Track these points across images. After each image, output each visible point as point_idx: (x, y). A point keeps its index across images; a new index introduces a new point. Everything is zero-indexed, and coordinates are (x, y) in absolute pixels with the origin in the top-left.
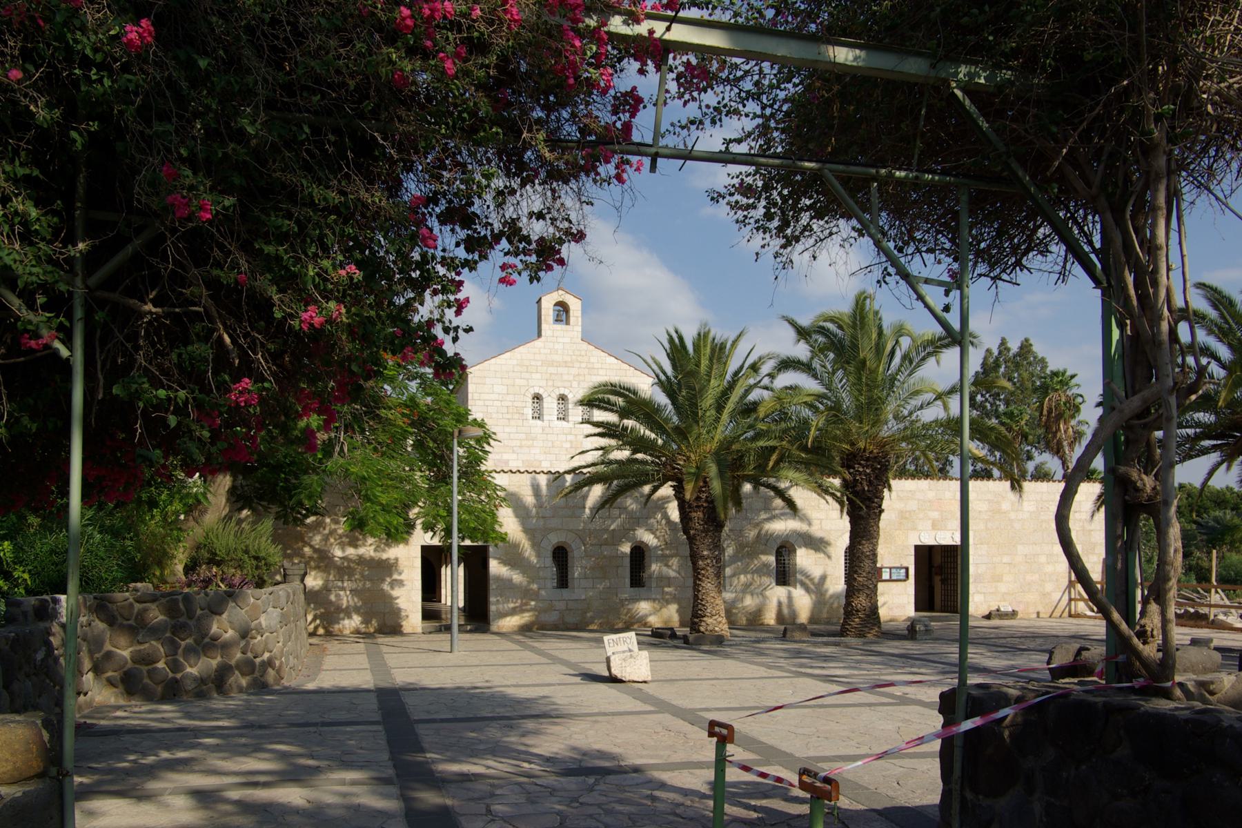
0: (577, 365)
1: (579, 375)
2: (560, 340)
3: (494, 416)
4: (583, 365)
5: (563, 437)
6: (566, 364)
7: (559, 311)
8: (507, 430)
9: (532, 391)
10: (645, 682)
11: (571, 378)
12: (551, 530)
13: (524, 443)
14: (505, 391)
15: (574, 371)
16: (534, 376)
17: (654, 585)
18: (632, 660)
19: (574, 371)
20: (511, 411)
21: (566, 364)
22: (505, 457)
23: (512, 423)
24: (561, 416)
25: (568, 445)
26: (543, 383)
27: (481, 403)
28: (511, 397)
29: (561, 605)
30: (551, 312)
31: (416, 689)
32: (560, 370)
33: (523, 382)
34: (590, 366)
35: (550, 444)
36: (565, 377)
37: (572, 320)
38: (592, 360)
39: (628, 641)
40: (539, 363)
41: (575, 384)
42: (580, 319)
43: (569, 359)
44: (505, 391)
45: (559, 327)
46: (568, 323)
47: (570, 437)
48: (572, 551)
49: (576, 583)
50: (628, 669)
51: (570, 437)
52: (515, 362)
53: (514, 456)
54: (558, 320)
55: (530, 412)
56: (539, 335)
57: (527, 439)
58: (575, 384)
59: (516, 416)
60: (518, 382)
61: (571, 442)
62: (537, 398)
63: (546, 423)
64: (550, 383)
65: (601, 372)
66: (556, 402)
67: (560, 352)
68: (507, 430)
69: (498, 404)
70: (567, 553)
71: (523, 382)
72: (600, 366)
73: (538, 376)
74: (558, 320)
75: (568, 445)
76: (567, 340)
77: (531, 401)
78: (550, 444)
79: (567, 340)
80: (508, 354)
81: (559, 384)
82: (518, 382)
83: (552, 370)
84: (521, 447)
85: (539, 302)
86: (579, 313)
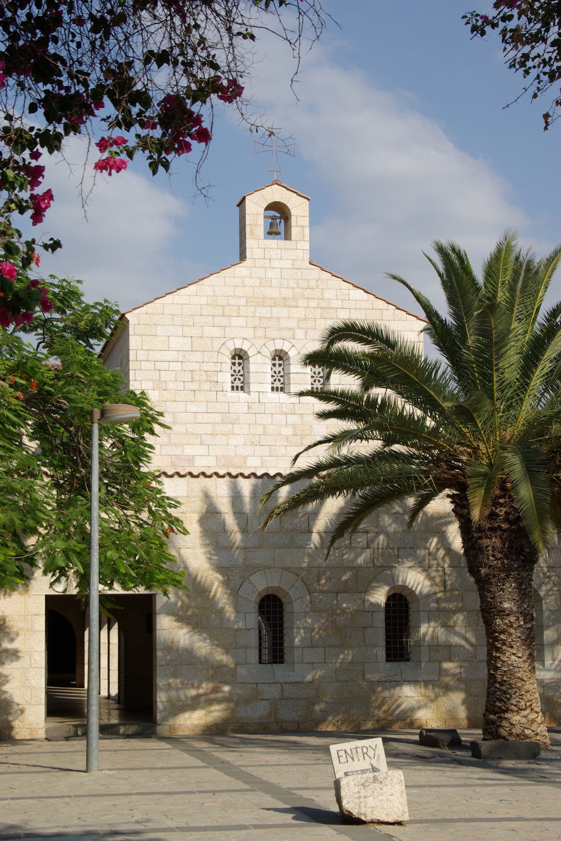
0: (302, 303)
1: (306, 319)
2: (275, 264)
3: (171, 386)
4: (313, 303)
5: (280, 419)
6: (285, 302)
7: (274, 218)
8: (192, 407)
9: (231, 346)
10: (399, 823)
11: (294, 324)
12: (257, 569)
13: (218, 428)
14: (188, 347)
15: (299, 313)
16: (235, 321)
17: (424, 658)
18: (376, 785)
19: (299, 313)
20: (197, 378)
21: (285, 302)
22: (189, 451)
23: (200, 396)
24: (278, 384)
25: (288, 431)
26: (249, 333)
27: (150, 366)
28: (197, 356)
29: (273, 692)
30: (261, 220)
31: (18, 836)
32: (276, 311)
33: (217, 332)
34: (323, 304)
35: (260, 430)
36: (284, 323)
37: (295, 231)
38: (328, 294)
39: (371, 753)
40: (243, 302)
41: (300, 334)
42: (307, 230)
43: (288, 293)
44: (188, 347)
45: (274, 243)
46: (287, 237)
47: (292, 419)
48: (291, 603)
49: (297, 654)
50: (371, 801)
52: (203, 300)
53: (202, 450)
54: (271, 233)
55: (229, 379)
56: (243, 257)
57: (223, 423)
58: (300, 334)
59: (206, 386)
60: (209, 331)
61: (294, 426)
63: (254, 397)
64: (260, 333)
66: (269, 362)
67: (275, 283)
68: (192, 407)
69: (177, 366)
70: (281, 606)
71: (217, 332)
73: (241, 321)
74: (271, 233)
75: (288, 431)
76: (287, 264)
77: (229, 361)
78: (260, 430)
79: (287, 264)
82: (209, 331)
83: (262, 312)
84: (213, 435)
85: (242, 203)
86: (306, 221)
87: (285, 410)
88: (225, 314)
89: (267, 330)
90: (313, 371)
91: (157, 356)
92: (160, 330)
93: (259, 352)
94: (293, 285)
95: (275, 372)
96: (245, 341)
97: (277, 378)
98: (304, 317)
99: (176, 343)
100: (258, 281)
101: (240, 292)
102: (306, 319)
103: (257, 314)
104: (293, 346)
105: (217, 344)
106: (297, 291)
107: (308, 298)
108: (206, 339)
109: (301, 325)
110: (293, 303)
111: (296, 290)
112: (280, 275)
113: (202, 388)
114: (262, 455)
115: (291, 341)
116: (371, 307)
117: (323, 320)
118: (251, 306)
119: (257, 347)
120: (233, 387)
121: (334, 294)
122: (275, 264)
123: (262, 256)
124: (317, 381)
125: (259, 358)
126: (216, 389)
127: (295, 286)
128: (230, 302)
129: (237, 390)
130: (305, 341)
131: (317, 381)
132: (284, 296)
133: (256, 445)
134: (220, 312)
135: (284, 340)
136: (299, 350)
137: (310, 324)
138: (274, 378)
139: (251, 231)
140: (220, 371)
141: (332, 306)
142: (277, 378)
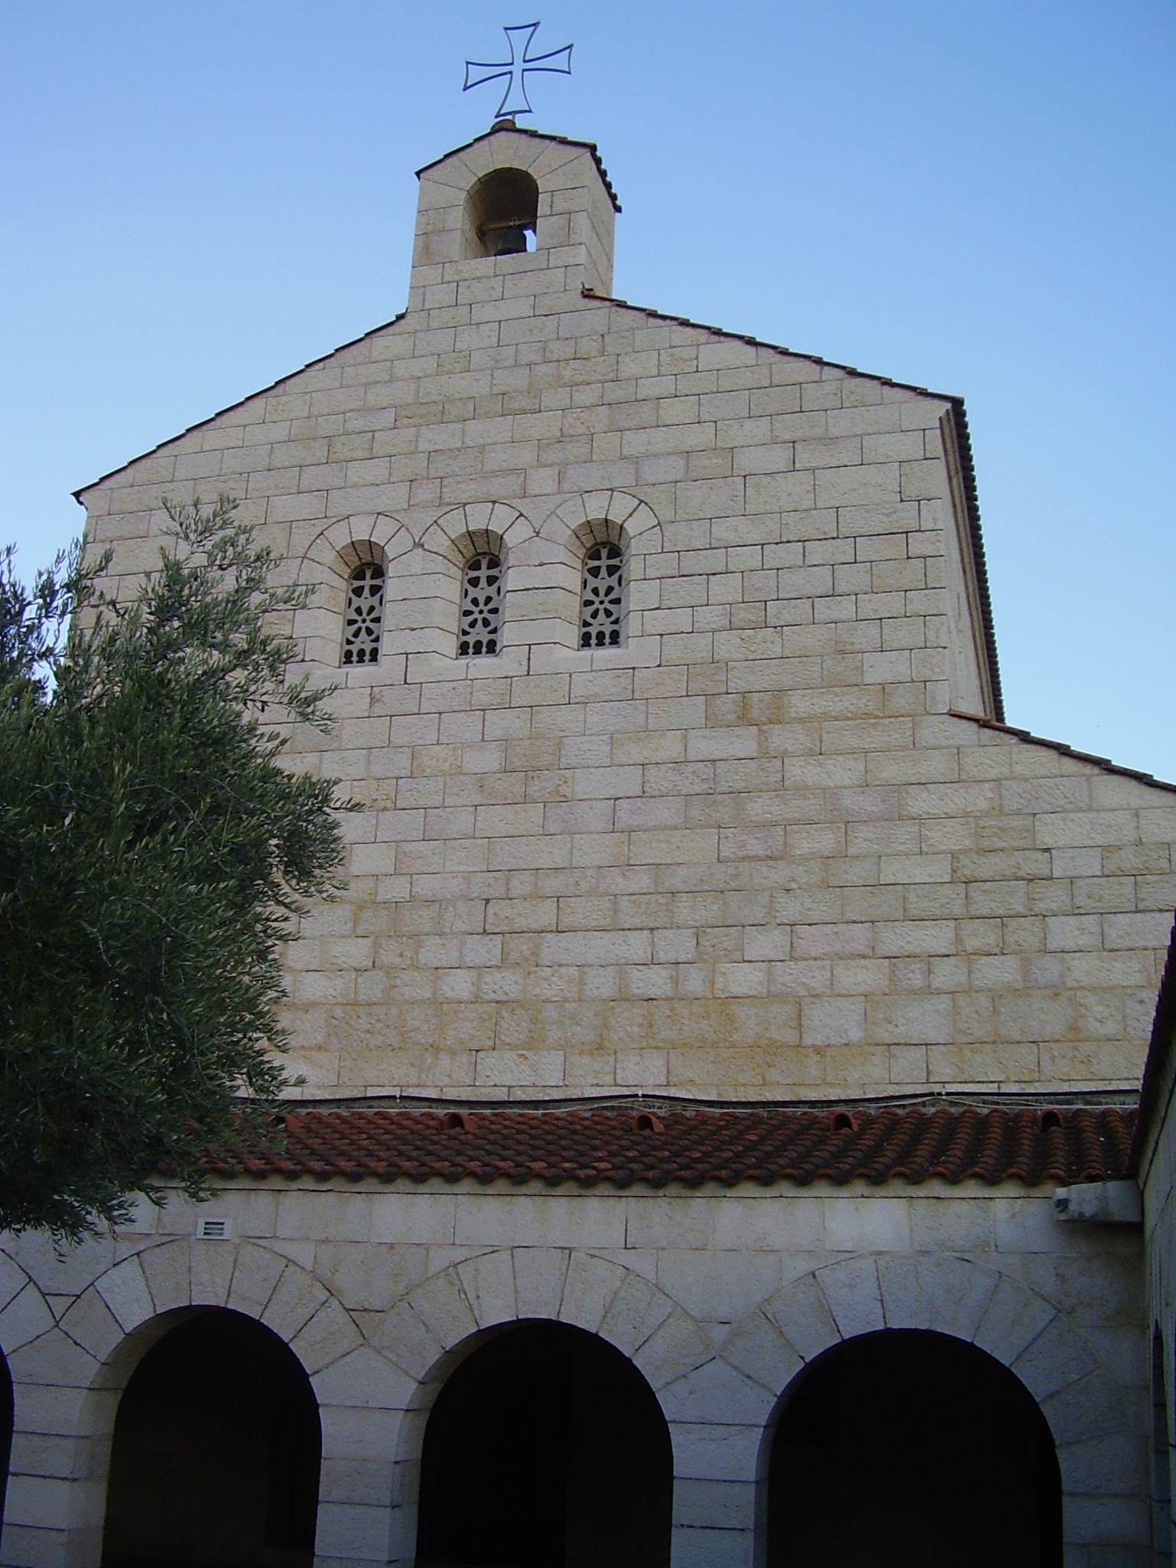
1: (563, 438)
2: (489, 313)
9: (341, 537)
16: (356, 473)
21: (505, 405)
26: (395, 497)
32: (476, 431)
33: (307, 506)
35: (401, 763)
36: (497, 459)
38: (630, 367)
40: (387, 418)
41: (542, 481)
43: (518, 380)
47: (500, 723)
51: (500, 723)
52: (280, 432)
58: (542, 481)
61: (506, 743)
65: (673, 411)
71: (307, 506)
72: (666, 385)
73: (376, 470)
75: (489, 760)
83: (437, 437)
87: (481, 698)
89: (446, 482)
90: (591, 585)
95: (475, 602)
97: (480, 617)
98: (559, 434)
100: (433, 362)
101: (379, 396)
102: (563, 438)
104: (521, 515)
106: (542, 369)
107: (574, 385)
108: (275, 528)
110: (525, 403)
111: (538, 368)
112: (495, 339)
114: (399, 837)
115: (516, 503)
116: (767, 382)
117: (614, 437)
119: (414, 531)
120: (348, 655)
121: (654, 361)
122: (489, 313)
123: (450, 299)
124: (602, 614)
125: (417, 561)
127: (536, 357)
128: (350, 427)
129: (361, 661)
130: (558, 499)
131: (602, 614)
132: (503, 389)
133: (385, 809)
134: (321, 455)
135: (494, 502)
136: (537, 526)
138: (470, 618)
141: (643, 393)
142: (476, 615)
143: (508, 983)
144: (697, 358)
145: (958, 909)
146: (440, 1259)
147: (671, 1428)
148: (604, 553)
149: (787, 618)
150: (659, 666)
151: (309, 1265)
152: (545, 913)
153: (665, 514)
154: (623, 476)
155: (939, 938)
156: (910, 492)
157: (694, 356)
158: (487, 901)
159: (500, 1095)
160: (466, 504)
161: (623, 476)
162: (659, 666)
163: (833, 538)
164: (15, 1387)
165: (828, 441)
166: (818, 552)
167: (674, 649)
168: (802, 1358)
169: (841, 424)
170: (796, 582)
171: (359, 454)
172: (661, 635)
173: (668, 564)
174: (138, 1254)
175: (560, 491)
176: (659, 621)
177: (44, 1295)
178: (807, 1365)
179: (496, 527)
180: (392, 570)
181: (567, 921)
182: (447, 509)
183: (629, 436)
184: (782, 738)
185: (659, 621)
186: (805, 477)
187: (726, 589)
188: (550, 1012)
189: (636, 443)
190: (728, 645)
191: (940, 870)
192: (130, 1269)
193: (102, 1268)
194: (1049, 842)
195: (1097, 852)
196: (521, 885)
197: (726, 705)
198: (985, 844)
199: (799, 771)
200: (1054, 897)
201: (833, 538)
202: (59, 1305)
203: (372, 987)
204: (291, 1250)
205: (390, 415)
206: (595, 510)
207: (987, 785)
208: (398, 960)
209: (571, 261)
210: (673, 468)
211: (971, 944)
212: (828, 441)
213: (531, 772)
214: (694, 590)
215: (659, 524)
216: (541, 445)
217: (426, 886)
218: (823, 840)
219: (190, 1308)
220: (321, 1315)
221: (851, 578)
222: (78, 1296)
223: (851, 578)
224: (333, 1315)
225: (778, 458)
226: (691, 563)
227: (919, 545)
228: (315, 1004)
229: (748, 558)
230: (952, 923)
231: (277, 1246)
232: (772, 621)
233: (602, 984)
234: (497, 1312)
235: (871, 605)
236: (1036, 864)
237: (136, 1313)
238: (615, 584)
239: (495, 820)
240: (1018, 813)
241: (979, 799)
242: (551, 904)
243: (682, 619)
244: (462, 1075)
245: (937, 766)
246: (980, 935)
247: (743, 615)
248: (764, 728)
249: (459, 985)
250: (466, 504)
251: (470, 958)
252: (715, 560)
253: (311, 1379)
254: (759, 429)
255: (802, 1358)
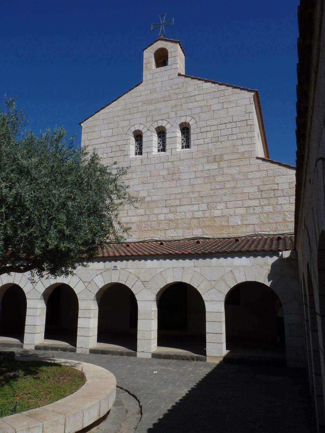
1: (176, 106)
2: (160, 80)
4: (180, 96)
6: (165, 100)
9: (133, 129)
15: (173, 103)
19: (173, 103)
21: (165, 100)
25: (164, 173)
28: (115, 139)
32: (159, 106)
33: (126, 123)
36: (163, 111)
38: (189, 89)
41: (173, 115)
43: (166, 94)
47: (166, 165)
52: (119, 108)
58: (173, 115)
60: (122, 124)
61: (168, 169)
62: (138, 136)
67: (158, 90)
69: (104, 146)
72: (197, 92)
73: (139, 115)
74: (158, 65)
75: (164, 173)
78: (148, 174)
80: (115, 103)
81: (158, 118)
82: (122, 124)
83: (150, 107)
87: (163, 160)
88: (130, 113)
91: (94, 142)
92: (97, 129)
93: (148, 130)
94: (169, 89)
96: (141, 125)
99: (104, 133)
100: (149, 91)
101: (139, 99)
103: (148, 109)
104: (169, 122)
105: (125, 130)
106: (171, 91)
109: (173, 110)
110: (169, 99)
113: (116, 155)
116: (217, 90)
117: (186, 105)
118: (145, 105)
122: (160, 80)
123: (151, 77)
125: (149, 133)
126: (124, 154)
132: (163, 96)
134: (128, 113)
137: (179, 108)
138: (160, 144)
139: (146, 67)
140: (127, 144)
141: (192, 94)
143: (171, 216)
144: (202, 86)
145: (259, 197)
146: (159, 271)
147: (205, 302)
148: (185, 129)
149: (223, 140)
150: (197, 151)
151: (134, 273)
152: (178, 202)
153: (197, 120)
154: (189, 113)
155: (255, 203)
156: (247, 111)
157: (202, 86)
158: (166, 200)
159: (171, 239)
160: (157, 121)
161: (189, 113)
162: (197, 151)
163: (231, 123)
164: (79, 301)
165: (230, 102)
166: (229, 126)
167: (201, 148)
168: (230, 287)
169: (232, 98)
170: (224, 132)
171: (136, 112)
172: (198, 145)
173: (198, 130)
174: (101, 273)
175: (176, 117)
176: (197, 142)
177: (83, 282)
178: (231, 289)
179: (163, 125)
180: (144, 135)
181: (182, 203)
182: (154, 122)
183: (190, 104)
184: (223, 164)
185: (197, 142)
186: (226, 110)
187: (210, 135)
188: (179, 222)
189: (191, 105)
190: (211, 146)
191: (255, 189)
192: (100, 276)
193: (94, 276)
194: (278, 182)
195: (288, 184)
196: (172, 197)
197: (211, 159)
198: (265, 183)
199: (226, 171)
200: (279, 193)
201: (231, 123)
202: (86, 284)
203: (145, 219)
204: (130, 270)
205: (141, 103)
206: (183, 120)
207: (264, 171)
208: (149, 213)
209: (176, 67)
210: (198, 110)
211: (262, 204)
212: (230, 102)
213: (174, 174)
214: (204, 135)
215: (196, 122)
216: (172, 107)
217: (155, 198)
218: (232, 184)
219: (112, 283)
220: (137, 283)
221: (235, 131)
222: (90, 282)
223: (235, 131)
224: (139, 283)
225: (220, 106)
226: (203, 130)
227: (249, 123)
228: (134, 222)
229: (214, 128)
230: (258, 200)
231: (128, 270)
232: (220, 141)
233: (189, 215)
234: (170, 281)
235: (239, 136)
236: (276, 187)
237: (101, 285)
238: (188, 135)
239: (167, 185)
240: (271, 177)
241: (264, 174)
242: (179, 200)
243: (202, 141)
244: (163, 235)
245: (254, 168)
246: (264, 202)
247: (214, 140)
248: (219, 162)
249: (162, 217)
250: (157, 121)
251: (163, 212)
252: (208, 129)
253: (135, 296)
254: (216, 101)
255: (230, 287)
